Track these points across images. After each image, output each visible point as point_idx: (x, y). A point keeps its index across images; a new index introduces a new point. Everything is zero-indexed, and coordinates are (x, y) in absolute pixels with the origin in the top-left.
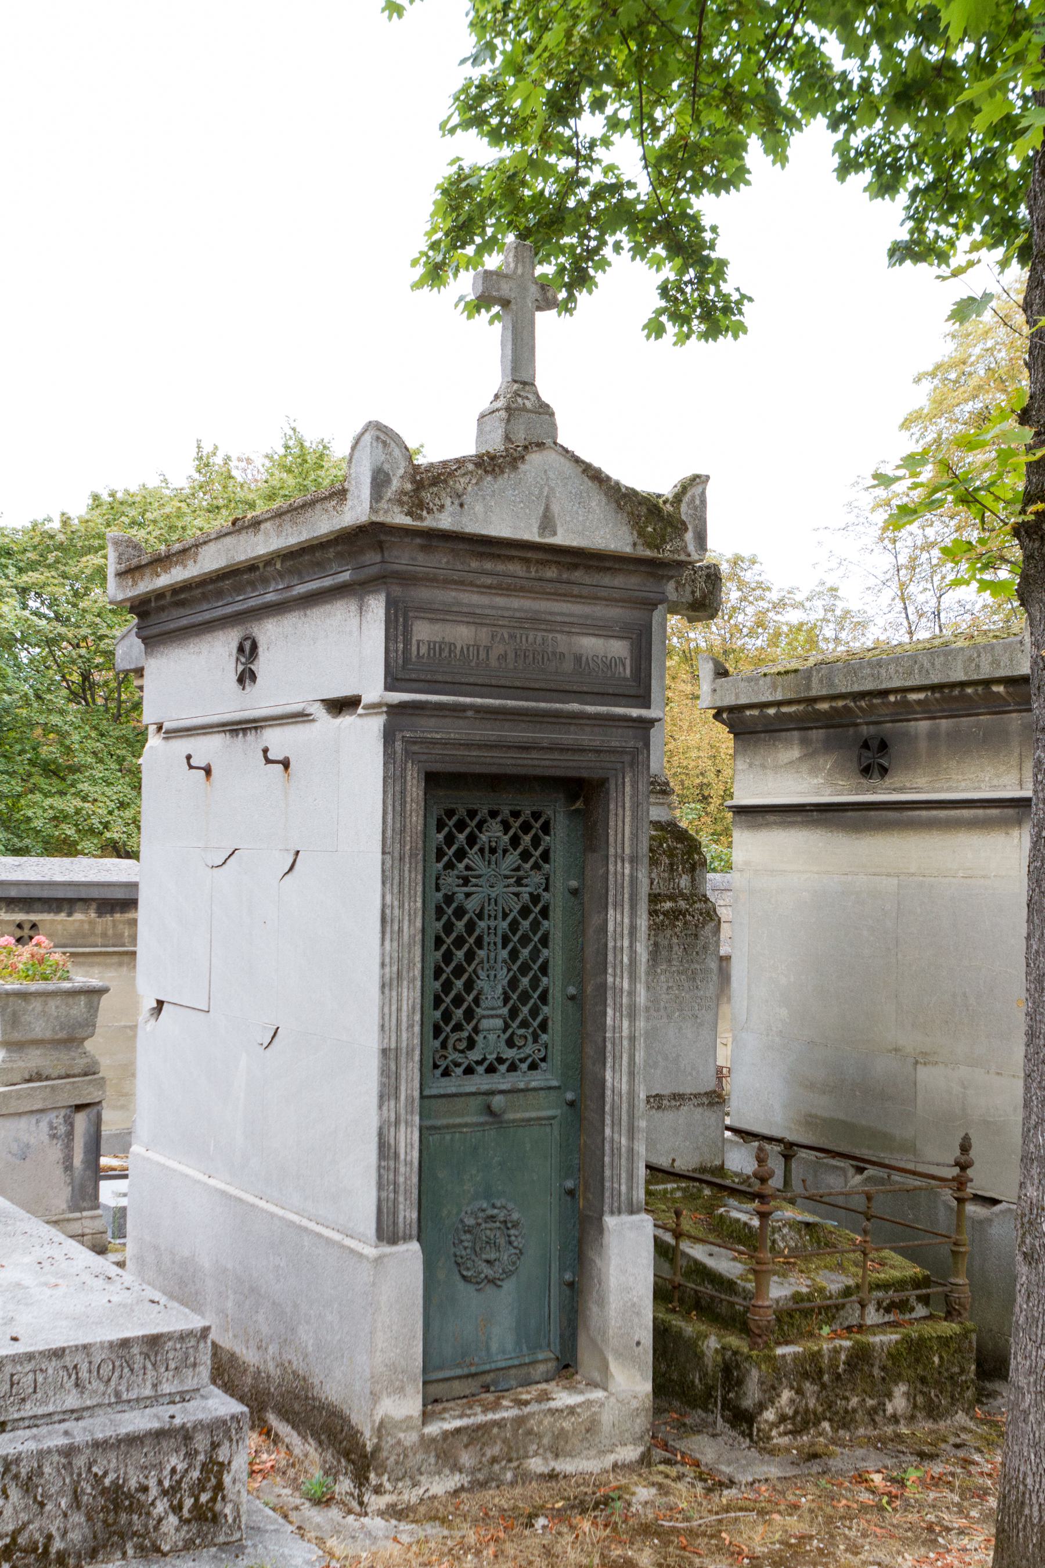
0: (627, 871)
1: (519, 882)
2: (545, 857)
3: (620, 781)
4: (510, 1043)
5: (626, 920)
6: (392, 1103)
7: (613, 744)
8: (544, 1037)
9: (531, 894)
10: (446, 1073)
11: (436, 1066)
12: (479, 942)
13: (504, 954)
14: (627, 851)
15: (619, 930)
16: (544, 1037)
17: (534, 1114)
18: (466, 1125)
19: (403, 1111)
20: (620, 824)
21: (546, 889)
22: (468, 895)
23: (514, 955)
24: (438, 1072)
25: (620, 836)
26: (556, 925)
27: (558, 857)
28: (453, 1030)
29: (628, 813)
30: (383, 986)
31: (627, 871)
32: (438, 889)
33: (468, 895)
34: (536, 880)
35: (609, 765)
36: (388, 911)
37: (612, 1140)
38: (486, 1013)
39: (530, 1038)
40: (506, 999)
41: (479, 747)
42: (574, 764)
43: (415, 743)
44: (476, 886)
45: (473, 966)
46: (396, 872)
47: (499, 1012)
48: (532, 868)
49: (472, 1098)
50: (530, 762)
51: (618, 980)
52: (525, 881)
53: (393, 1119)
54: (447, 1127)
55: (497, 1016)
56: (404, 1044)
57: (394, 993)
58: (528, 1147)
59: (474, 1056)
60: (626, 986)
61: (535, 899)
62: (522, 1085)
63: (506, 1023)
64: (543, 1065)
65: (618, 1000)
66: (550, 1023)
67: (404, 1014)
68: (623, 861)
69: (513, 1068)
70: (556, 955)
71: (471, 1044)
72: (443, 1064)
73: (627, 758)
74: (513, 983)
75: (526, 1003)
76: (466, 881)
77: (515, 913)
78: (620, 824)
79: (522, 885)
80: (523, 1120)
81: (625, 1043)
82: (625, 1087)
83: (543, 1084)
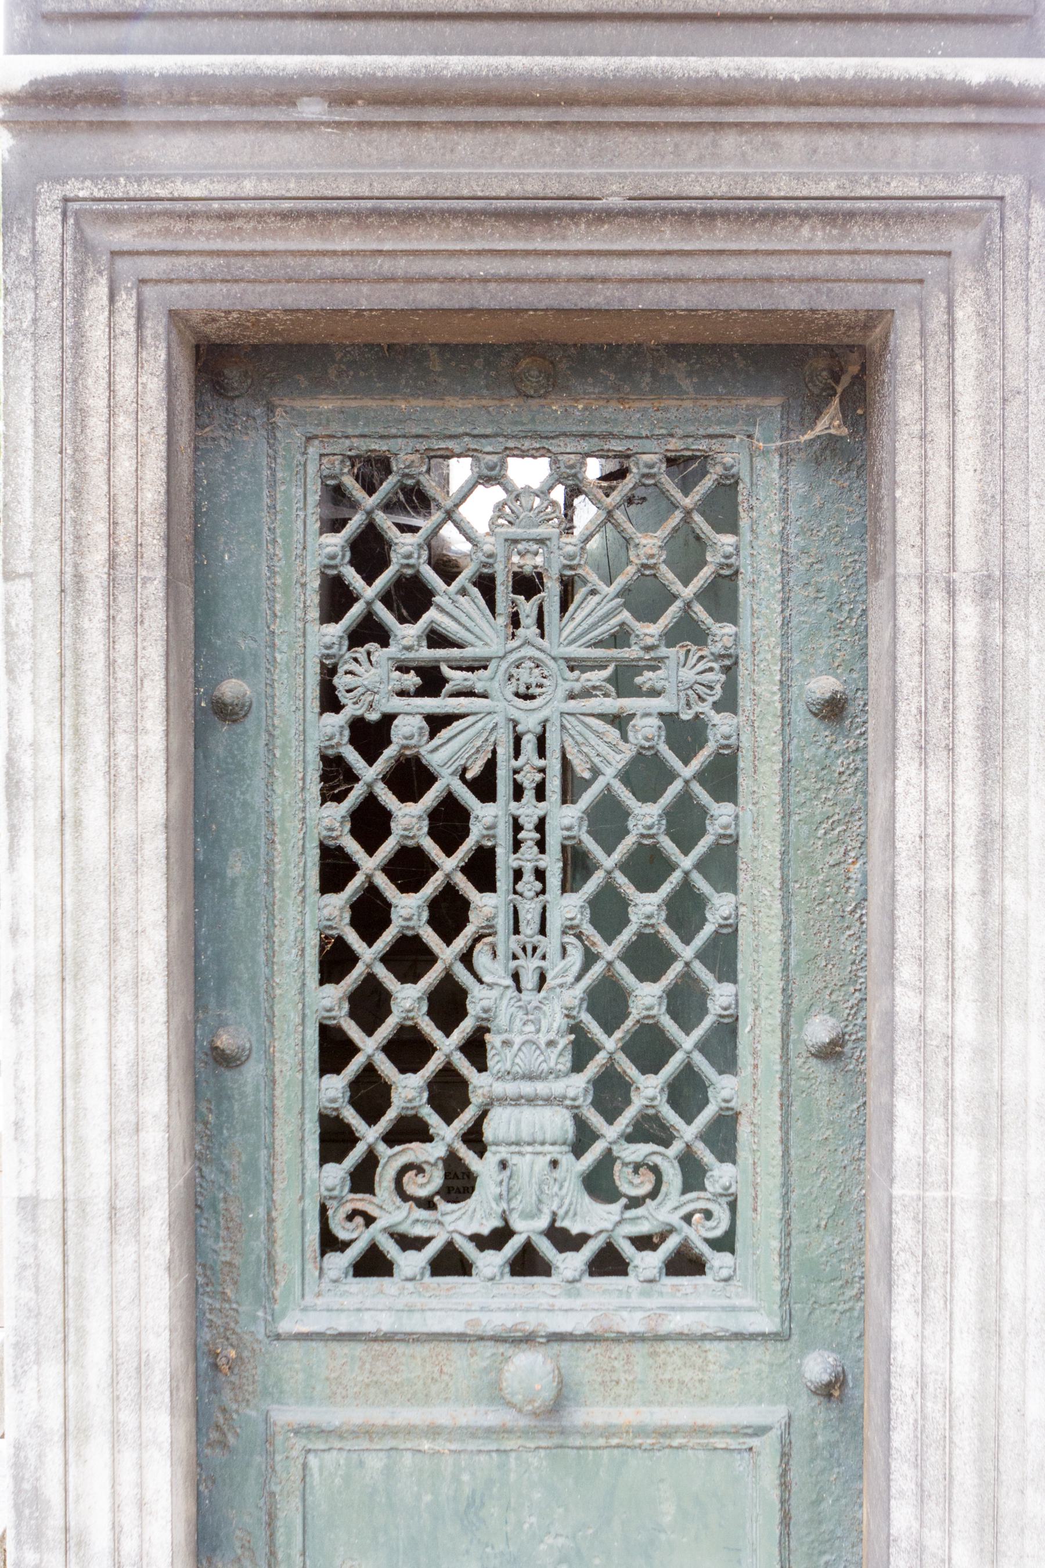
0: (968, 630)
1: (624, 681)
2: (722, 596)
3: (937, 320)
4: (599, 1184)
5: (968, 801)
6: (52, 1371)
7: (896, 188)
8: (721, 1175)
9: (668, 719)
10: (373, 1264)
11: (330, 1243)
12: (482, 869)
13: (569, 907)
14: (968, 558)
15: (938, 832)
16: (721, 1175)
17: (682, 1415)
18: (434, 1431)
19: (98, 1399)
20: (939, 465)
21: (728, 703)
22: (437, 723)
23: (608, 912)
24: (340, 1262)
25: (938, 510)
26: (754, 818)
27: (760, 599)
28: (391, 1138)
29: (968, 428)
30: (17, 997)
31: (968, 630)
32: (330, 702)
33: (437, 723)
34: (688, 675)
35: (891, 267)
36: (26, 761)
37: (919, 1548)
38: (511, 1088)
39: (673, 1176)
40: (582, 1050)
41: (359, 219)
42: (747, 267)
43: (114, 218)
44: (470, 693)
45: (460, 943)
46: (49, 636)
47: (557, 1087)
48: (671, 638)
49: (458, 1348)
50: (565, 266)
51: (937, 1004)
52: (646, 679)
53: (54, 1422)
54: (368, 1432)
55: (549, 1100)
56: (98, 1187)
57: (51, 1025)
58: (668, 1512)
59: (461, 1222)
60: (967, 1025)
61: (685, 734)
62: (633, 1323)
63: (581, 1124)
64: (718, 1261)
65: (938, 1073)
66: (744, 1130)
67: (95, 1095)
68: (951, 592)
69: (609, 1262)
70: (754, 908)
71: (459, 1184)
72: (360, 1238)
73: (962, 240)
74: (607, 1002)
75: (651, 1065)
76: (432, 682)
77: (609, 776)
78: (939, 465)
79: (637, 692)
80: (641, 1431)
81: (967, 1223)
82: (965, 1376)
83: (711, 1323)
